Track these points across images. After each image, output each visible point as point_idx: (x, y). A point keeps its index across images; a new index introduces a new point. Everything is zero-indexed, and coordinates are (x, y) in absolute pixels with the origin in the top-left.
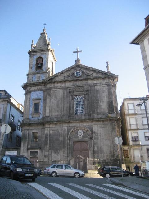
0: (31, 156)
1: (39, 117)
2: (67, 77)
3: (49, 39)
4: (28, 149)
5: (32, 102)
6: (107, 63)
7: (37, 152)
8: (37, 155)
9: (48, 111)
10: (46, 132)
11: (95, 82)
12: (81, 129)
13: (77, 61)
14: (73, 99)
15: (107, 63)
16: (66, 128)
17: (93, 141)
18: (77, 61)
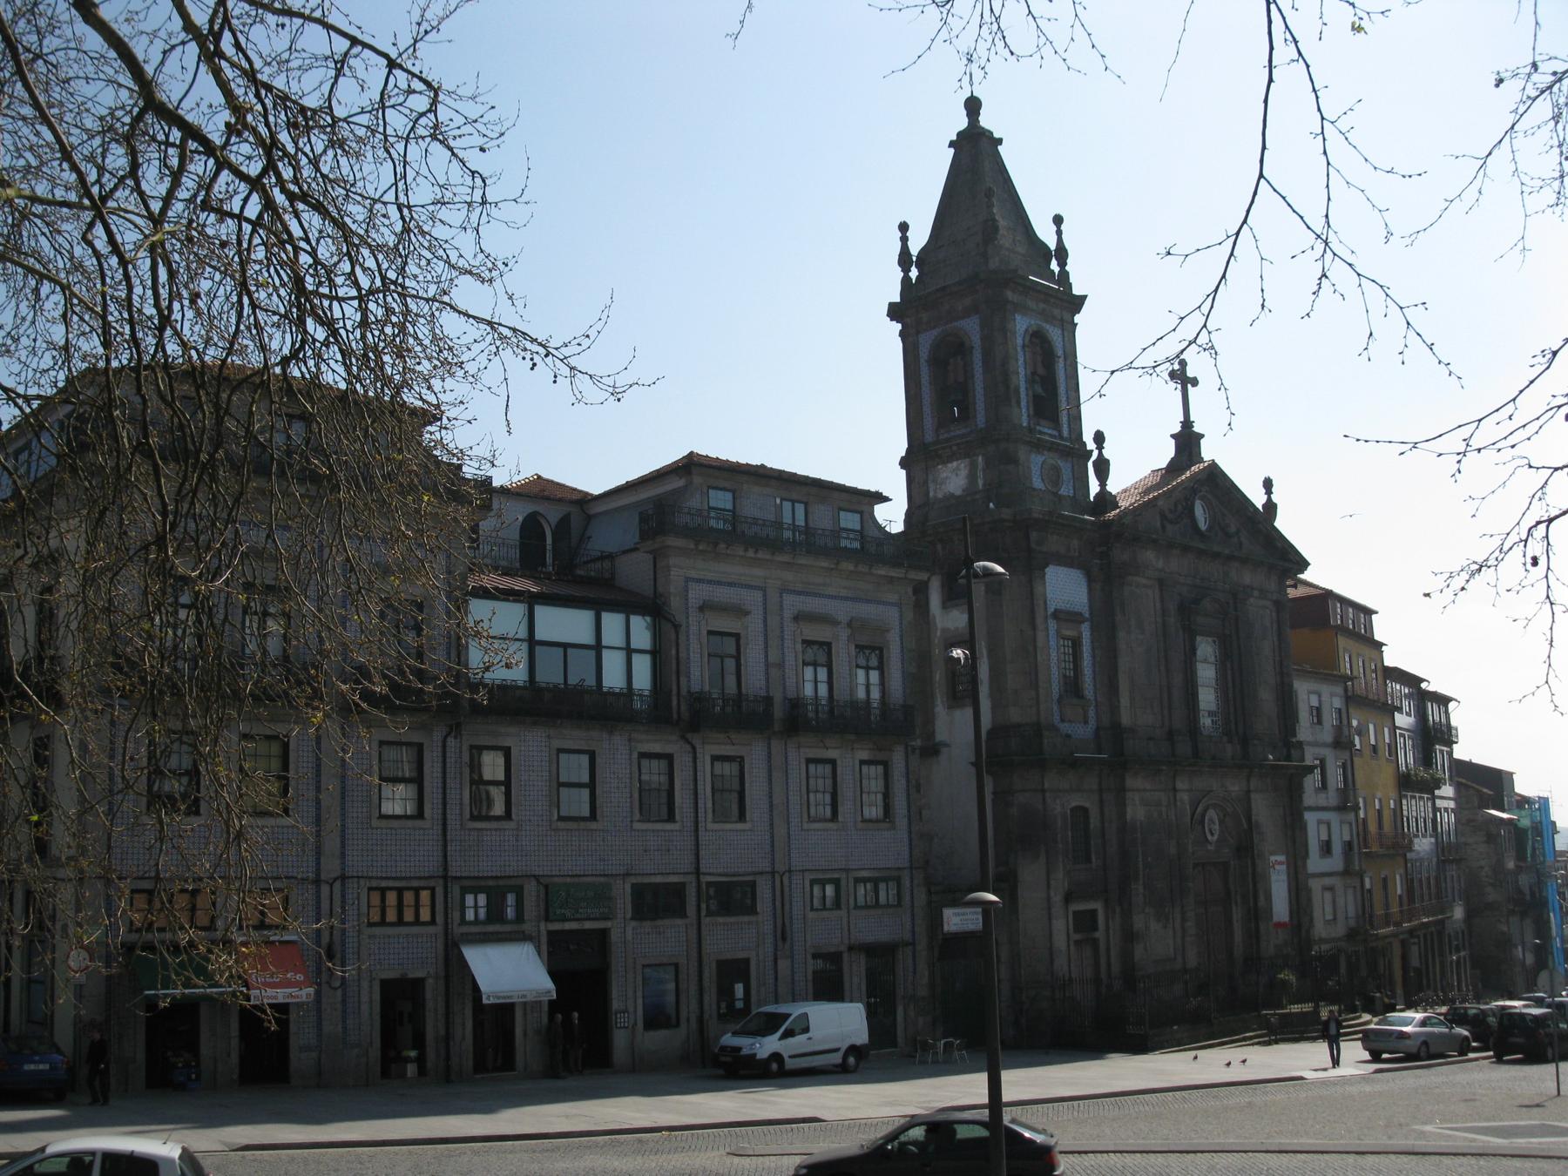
0: (1078, 937)
1: (1086, 722)
2: (1171, 522)
3: (1058, 220)
4: (1068, 898)
5: (1052, 625)
6: (1268, 484)
7: (1094, 912)
8: (1095, 929)
9: (1124, 701)
10: (1128, 817)
11: (1247, 577)
12: (1215, 806)
13: (1187, 440)
14: (1193, 650)
15: (1268, 484)
16: (1185, 797)
17: (1254, 864)
18: (1187, 440)
